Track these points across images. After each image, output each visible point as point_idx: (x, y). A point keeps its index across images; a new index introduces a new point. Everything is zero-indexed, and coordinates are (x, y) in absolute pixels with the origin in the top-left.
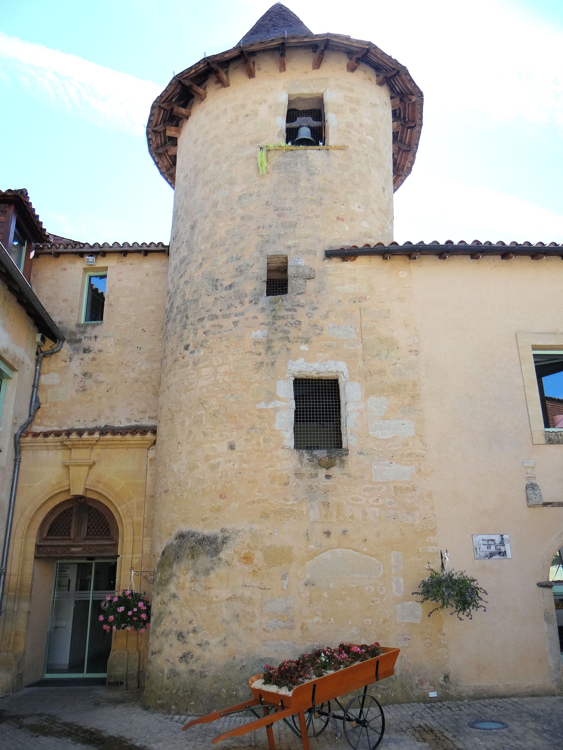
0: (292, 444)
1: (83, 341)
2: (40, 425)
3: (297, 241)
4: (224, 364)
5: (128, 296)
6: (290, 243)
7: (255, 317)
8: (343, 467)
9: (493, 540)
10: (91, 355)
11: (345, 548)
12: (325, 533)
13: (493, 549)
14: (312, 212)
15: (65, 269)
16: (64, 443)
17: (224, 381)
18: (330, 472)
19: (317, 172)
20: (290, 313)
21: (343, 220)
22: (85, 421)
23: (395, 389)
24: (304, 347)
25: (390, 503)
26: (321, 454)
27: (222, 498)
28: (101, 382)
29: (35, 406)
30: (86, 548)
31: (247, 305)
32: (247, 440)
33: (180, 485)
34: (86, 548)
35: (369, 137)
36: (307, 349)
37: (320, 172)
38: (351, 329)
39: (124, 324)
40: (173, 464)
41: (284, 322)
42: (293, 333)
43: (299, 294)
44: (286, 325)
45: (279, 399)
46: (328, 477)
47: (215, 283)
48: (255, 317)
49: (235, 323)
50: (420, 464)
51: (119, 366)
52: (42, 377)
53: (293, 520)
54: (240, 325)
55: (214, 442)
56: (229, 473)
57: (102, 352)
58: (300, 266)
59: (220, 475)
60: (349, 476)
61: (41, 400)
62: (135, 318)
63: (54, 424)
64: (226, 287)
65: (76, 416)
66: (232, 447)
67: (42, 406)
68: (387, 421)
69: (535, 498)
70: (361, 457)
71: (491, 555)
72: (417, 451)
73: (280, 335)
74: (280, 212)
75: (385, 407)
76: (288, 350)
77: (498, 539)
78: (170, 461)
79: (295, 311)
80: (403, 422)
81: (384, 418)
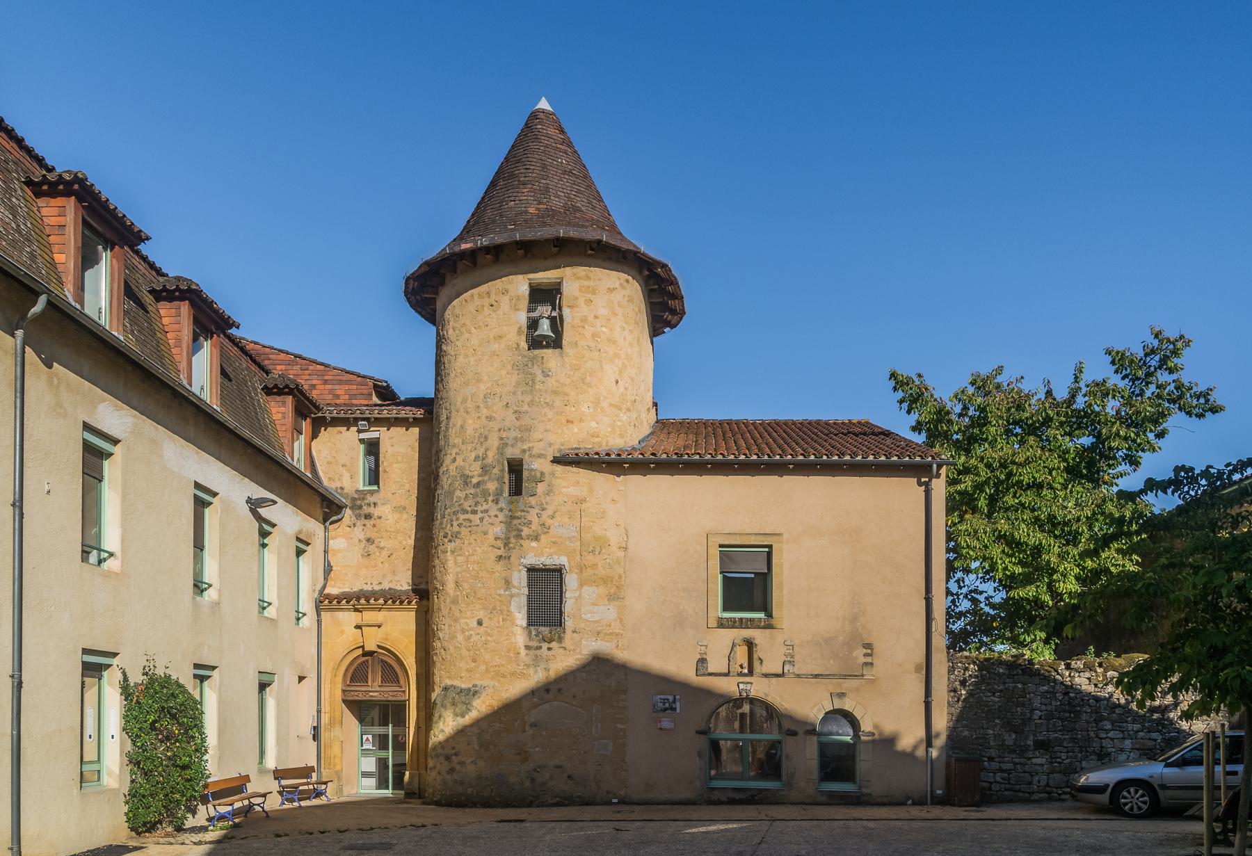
0: (524, 623)
24: (534, 544)
26: (545, 630)
35: (604, 329)
42: (526, 531)
46: (549, 649)
47: (466, 480)
49: (481, 519)
66: (480, 623)
81: (593, 604)
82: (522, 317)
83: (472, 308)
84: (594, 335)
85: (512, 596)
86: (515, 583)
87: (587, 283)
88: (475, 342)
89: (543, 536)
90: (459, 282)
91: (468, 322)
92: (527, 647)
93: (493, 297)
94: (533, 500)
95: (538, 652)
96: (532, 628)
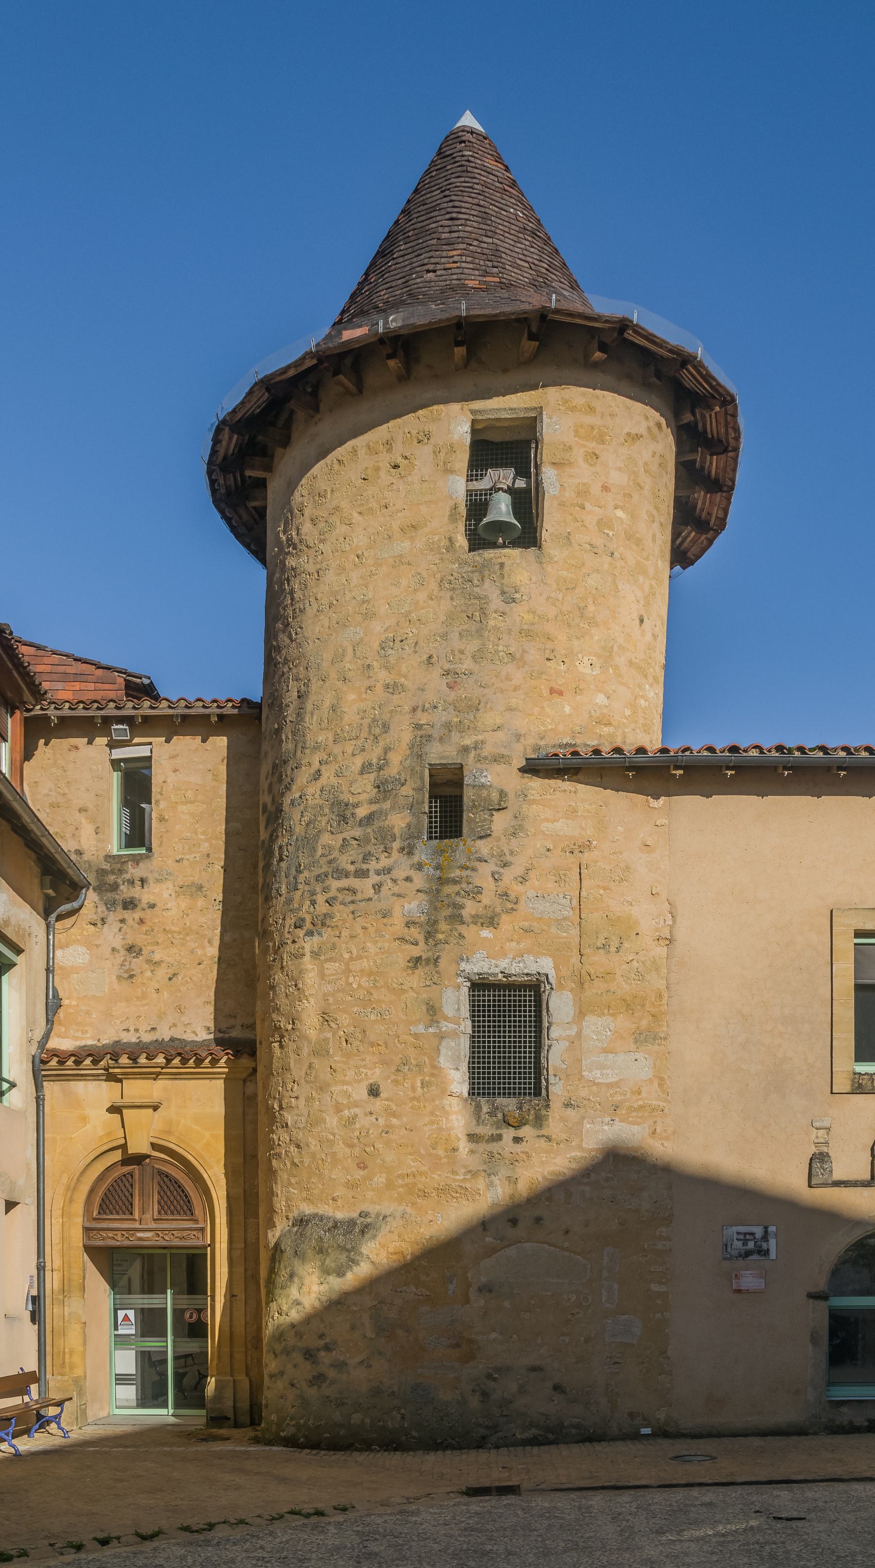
0: (465, 1089)
1: (122, 887)
2: (65, 1036)
3: (480, 737)
4: (359, 957)
5: (191, 802)
6: (468, 741)
7: (408, 879)
8: (541, 1126)
9: (752, 1234)
10: (137, 915)
11: (538, 1242)
12: (509, 1220)
13: (751, 1245)
14: (507, 679)
15: (77, 748)
16: (111, 1070)
17: (360, 986)
18: (521, 1133)
19: (517, 596)
20: (464, 873)
21: (561, 693)
22: (137, 1030)
23: (629, 1005)
24: (486, 933)
25: (607, 1180)
26: (509, 1104)
27: (360, 1168)
28: (158, 963)
29: (53, 1005)
30: (159, 1233)
31: (395, 854)
32: (396, 1082)
33: (298, 1146)
34: (159, 1233)
36: (490, 936)
37: (524, 597)
38: (563, 901)
39: (188, 857)
40: (286, 1114)
41: (457, 888)
42: (470, 908)
43: (481, 838)
44: (458, 894)
45: (446, 1019)
46: (517, 1140)
47: (343, 813)
48: (408, 879)
49: (377, 887)
50: (655, 1122)
51: (187, 934)
52: (59, 953)
53: (464, 1202)
54: (384, 889)
55: (348, 1083)
56: (371, 1132)
57: (156, 908)
58: (483, 786)
59: (357, 1133)
60: (549, 1139)
61: (61, 995)
62: (207, 845)
63: (88, 1035)
64: (361, 821)
65: (121, 1022)
66: (374, 1092)
67: (65, 1002)
68: (611, 1056)
69: (822, 1174)
70: (569, 1111)
71: (748, 1253)
72: (653, 1102)
73: (448, 912)
74: (452, 677)
75: (609, 1033)
76: (461, 936)
77: (758, 1231)
78: (281, 1108)
79: (474, 869)
80: (637, 1057)
81: (606, 1051)
82: (458, 486)
83: (352, 473)
84: (603, 524)
85: (441, 1037)
86: (449, 1010)
87: (588, 420)
88: (360, 539)
89: (504, 917)
90: (325, 428)
91: (343, 504)
92: (473, 1138)
93: (399, 448)
94: (483, 847)
95: (494, 1147)
96: (483, 1100)
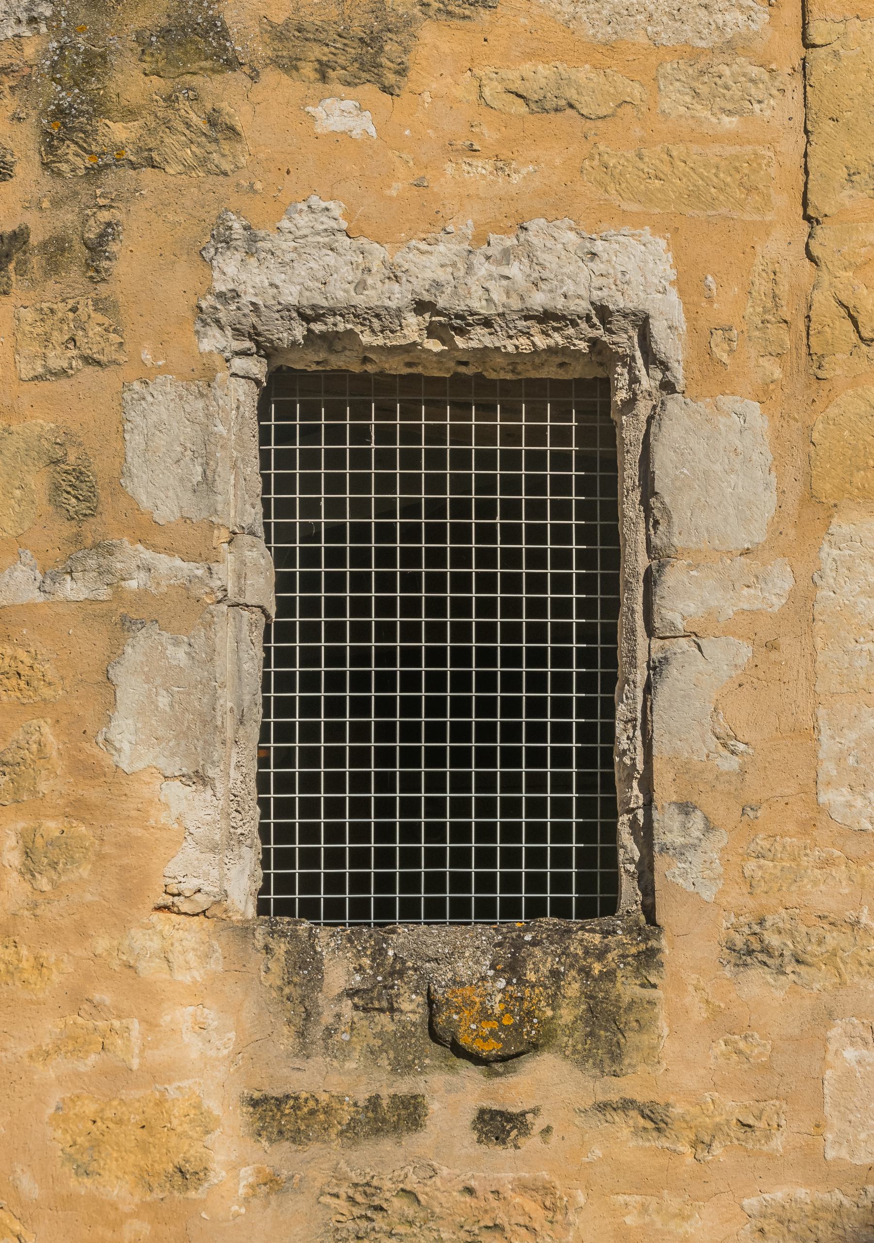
8: (616, 1055)
18: (518, 1089)
36: (363, 125)
45: (147, 531)
46: (498, 1126)
60: (655, 1118)
76: (221, 128)
85: (123, 621)
86: (158, 489)
95: (385, 1160)
